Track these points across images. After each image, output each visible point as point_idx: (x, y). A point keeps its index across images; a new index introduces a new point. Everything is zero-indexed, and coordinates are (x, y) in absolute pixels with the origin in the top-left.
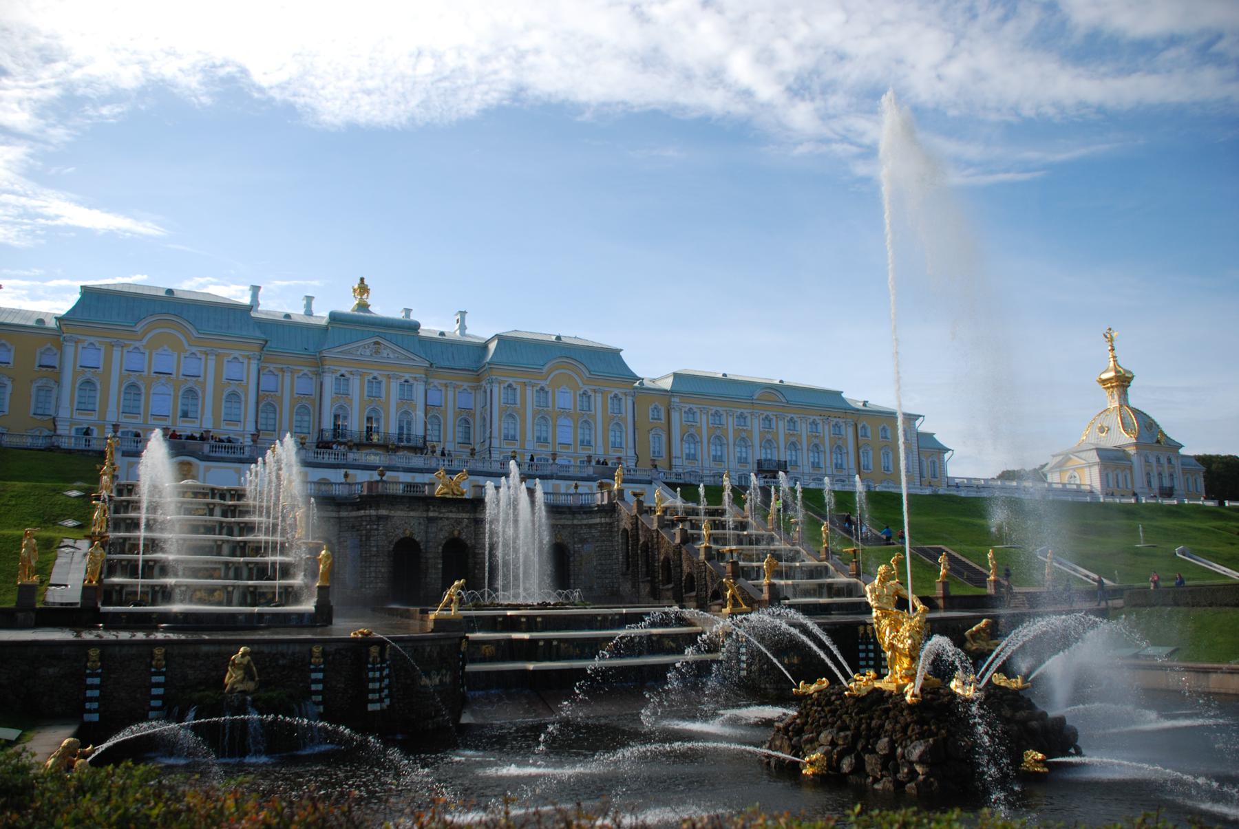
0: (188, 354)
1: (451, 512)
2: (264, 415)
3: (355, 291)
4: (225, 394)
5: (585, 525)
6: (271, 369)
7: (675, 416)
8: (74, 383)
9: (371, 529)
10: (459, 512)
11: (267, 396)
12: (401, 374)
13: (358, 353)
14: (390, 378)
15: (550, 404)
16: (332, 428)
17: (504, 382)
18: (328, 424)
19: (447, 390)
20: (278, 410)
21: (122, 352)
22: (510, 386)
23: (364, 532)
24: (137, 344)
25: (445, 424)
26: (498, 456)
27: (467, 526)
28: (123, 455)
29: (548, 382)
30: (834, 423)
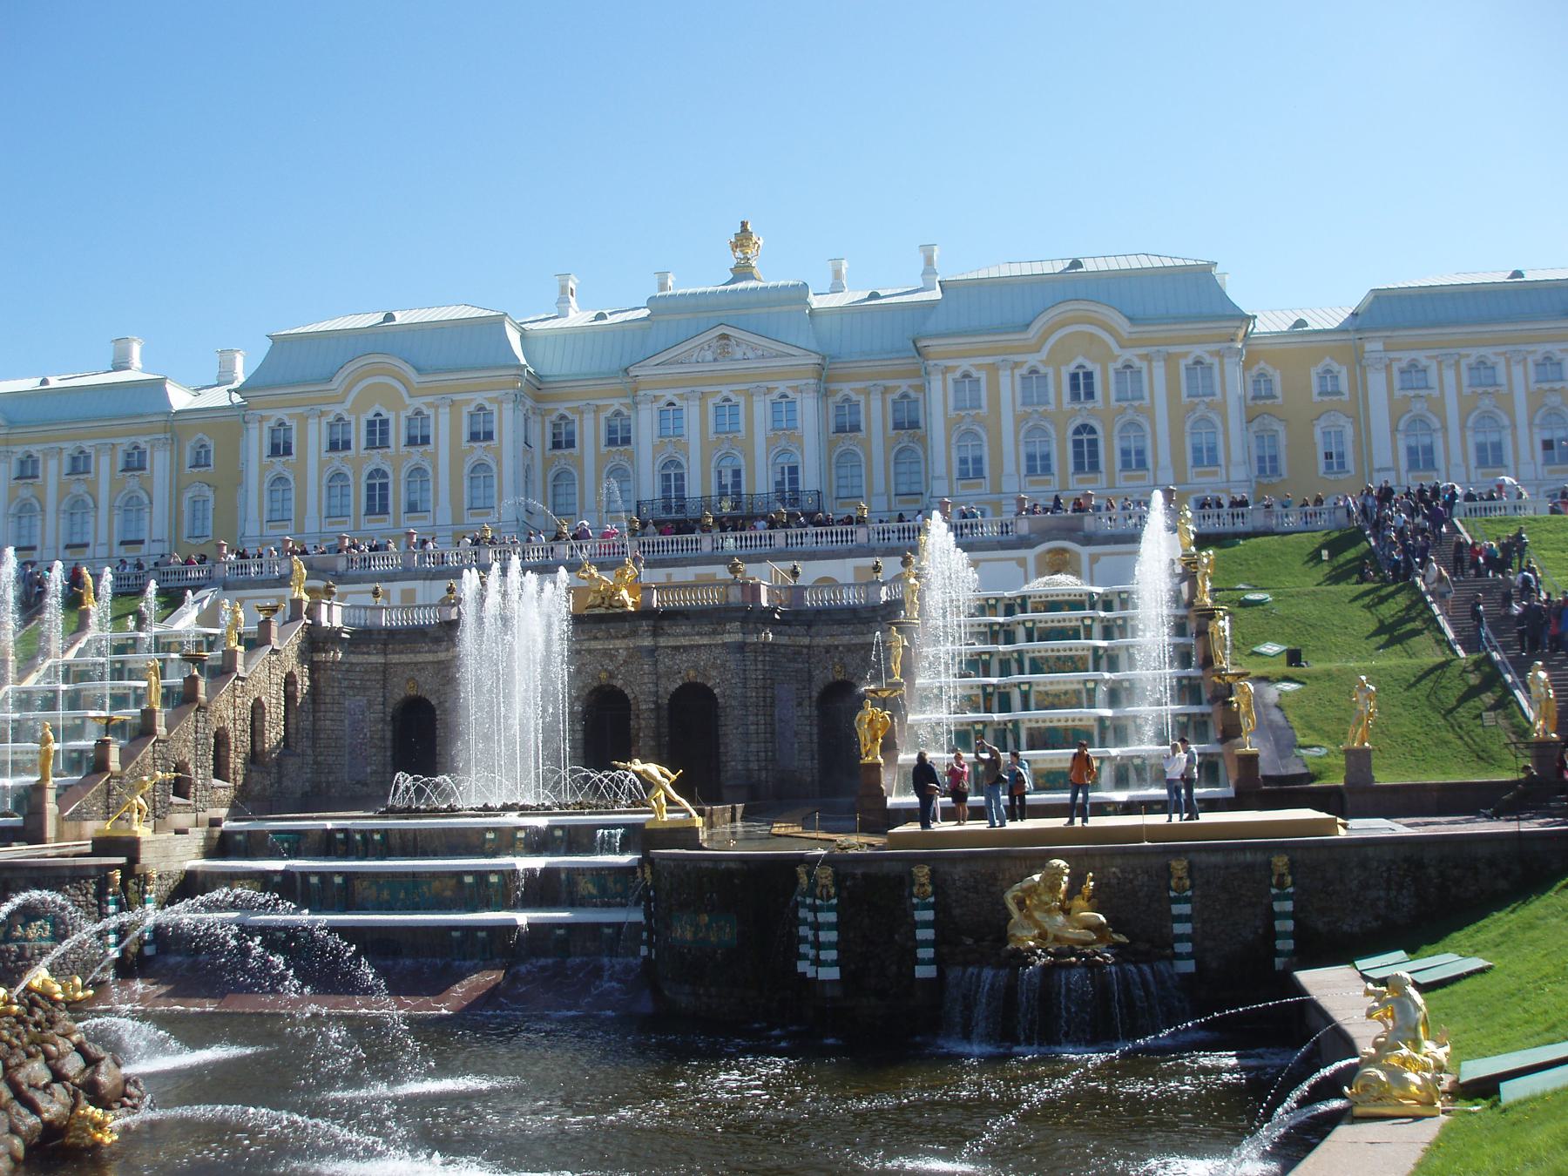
0: (410, 412)
1: (596, 638)
4: (466, 470)
7: (1377, 384)
8: (261, 484)
10: (610, 637)
11: (558, 457)
12: (770, 385)
14: (752, 395)
16: (658, 495)
17: (953, 369)
18: (649, 488)
21: (320, 423)
22: (966, 375)
24: (338, 409)
27: (625, 661)
28: (225, 588)
29: (1043, 355)
30: (1404, 364)
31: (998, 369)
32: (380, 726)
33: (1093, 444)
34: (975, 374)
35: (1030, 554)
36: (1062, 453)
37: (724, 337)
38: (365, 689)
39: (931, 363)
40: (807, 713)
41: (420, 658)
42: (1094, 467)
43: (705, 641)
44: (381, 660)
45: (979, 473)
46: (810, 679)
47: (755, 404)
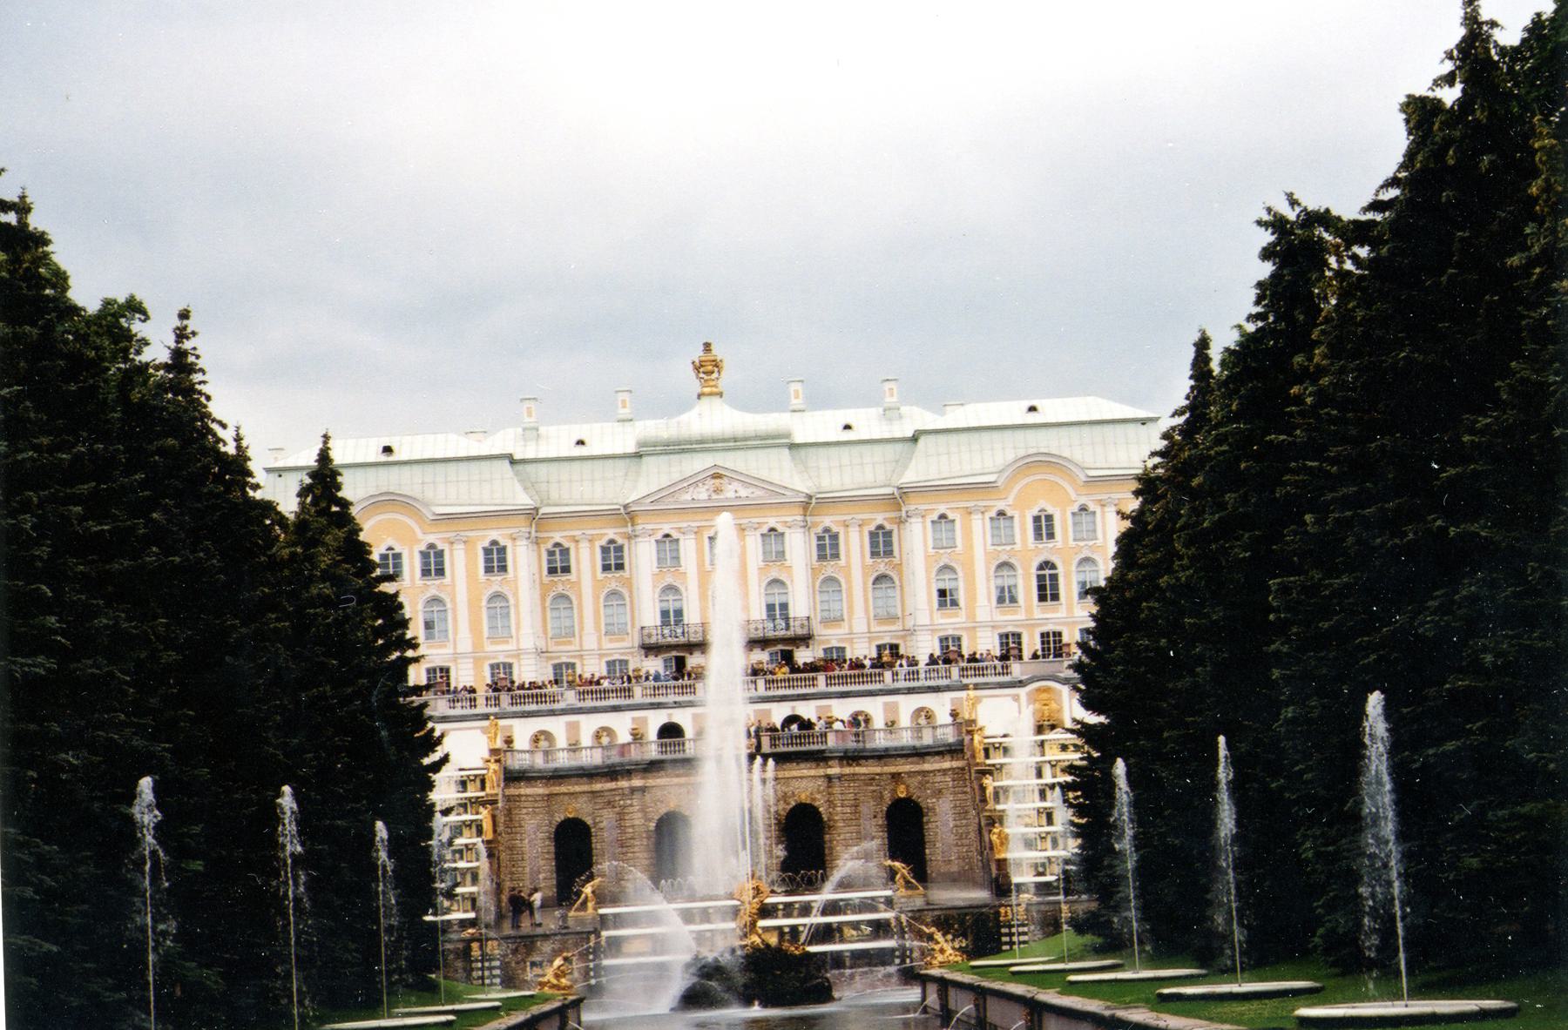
2: (556, 614)
3: (698, 367)
5: (939, 771)
6: (558, 539)
9: (625, 807)
13: (688, 497)
14: (744, 530)
15: (1018, 538)
16: (659, 623)
18: (649, 616)
19: (847, 533)
20: (575, 602)
23: (617, 809)
25: (850, 589)
26: (930, 638)
29: (1010, 500)
31: (970, 513)
32: (547, 843)
33: (1054, 578)
34: (951, 516)
35: (1022, 692)
36: (1027, 588)
37: (717, 476)
38: (538, 814)
39: (912, 507)
40: (880, 823)
41: (577, 789)
42: (1055, 597)
43: (813, 772)
44: (547, 792)
45: (954, 603)
46: (882, 797)
47: (747, 538)
